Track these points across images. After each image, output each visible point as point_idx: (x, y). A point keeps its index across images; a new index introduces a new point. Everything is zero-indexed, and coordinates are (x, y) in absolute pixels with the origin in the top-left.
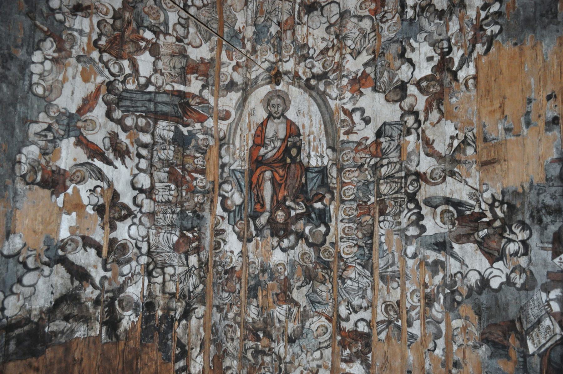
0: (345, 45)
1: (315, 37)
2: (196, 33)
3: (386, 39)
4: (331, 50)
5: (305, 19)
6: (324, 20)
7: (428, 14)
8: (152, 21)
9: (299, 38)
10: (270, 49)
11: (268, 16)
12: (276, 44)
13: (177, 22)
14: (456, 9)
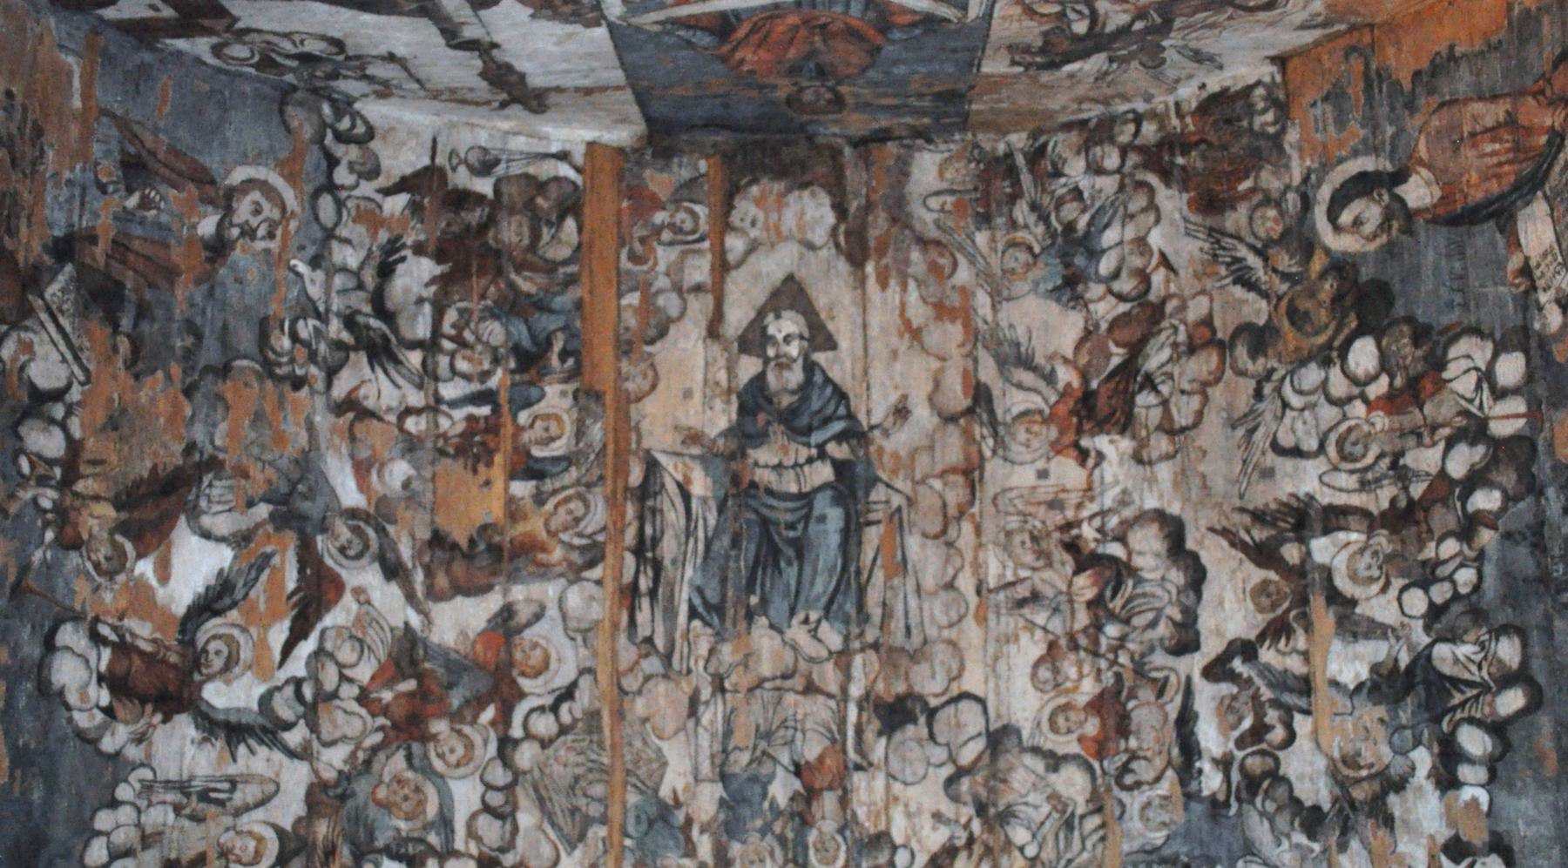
0: (1008, 843)
1: (913, 808)
2: (540, 828)
3: (1136, 845)
4: (963, 855)
5: (878, 749)
6: (939, 754)
7: (1270, 807)
8: (402, 825)
9: (861, 812)
10: (772, 854)
11: (763, 745)
12: (790, 835)
13: (477, 805)
14: (1362, 818)
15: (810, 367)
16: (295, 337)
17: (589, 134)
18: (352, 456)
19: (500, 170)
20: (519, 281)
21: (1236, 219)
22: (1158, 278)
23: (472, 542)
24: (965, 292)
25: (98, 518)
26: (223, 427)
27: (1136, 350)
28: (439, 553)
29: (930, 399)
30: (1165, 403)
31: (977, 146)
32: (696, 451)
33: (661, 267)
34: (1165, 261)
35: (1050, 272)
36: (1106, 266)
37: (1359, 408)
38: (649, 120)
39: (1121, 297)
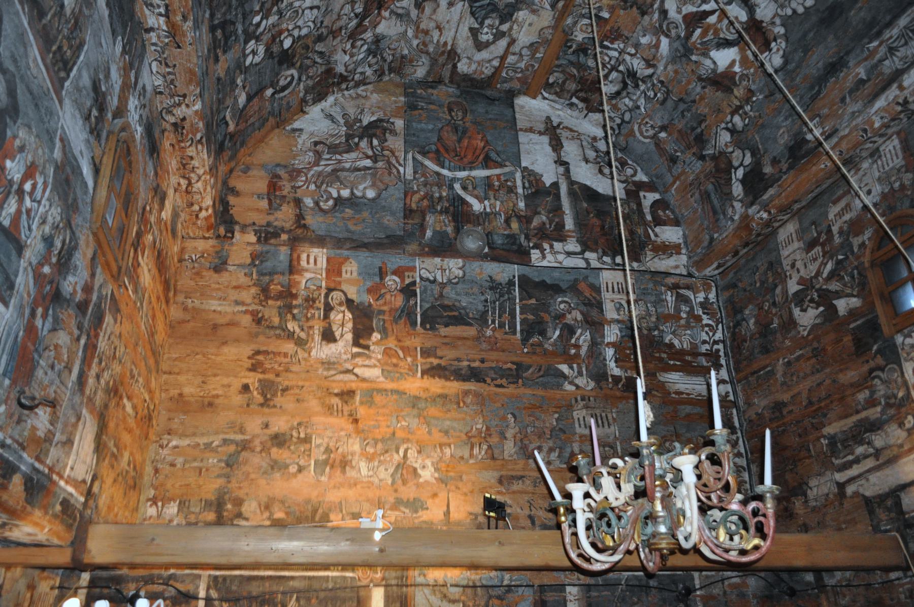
15: (482, 24)
16: (656, 95)
17: (533, 102)
18: (658, 52)
19: (567, 102)
20: (576, 72)
21: (321, 69)
22: (349, 46)
23: (631, 7)
24: (417, 37)
25: (739, 92)
26: (690, 87)
27: (360, 25)
28: (645, 9)
29: (438, 6)
30: (353, 10)
31: (401, 78)
32: (535, 7)
33: (524, 62)
34: (345, 52)
35: (382, 45)
36: (366, 47)
37: (290, 27)
38: (512, 106)
39: (362, 39)
